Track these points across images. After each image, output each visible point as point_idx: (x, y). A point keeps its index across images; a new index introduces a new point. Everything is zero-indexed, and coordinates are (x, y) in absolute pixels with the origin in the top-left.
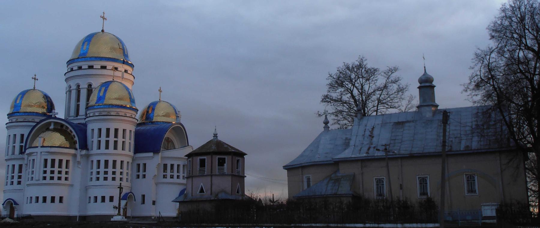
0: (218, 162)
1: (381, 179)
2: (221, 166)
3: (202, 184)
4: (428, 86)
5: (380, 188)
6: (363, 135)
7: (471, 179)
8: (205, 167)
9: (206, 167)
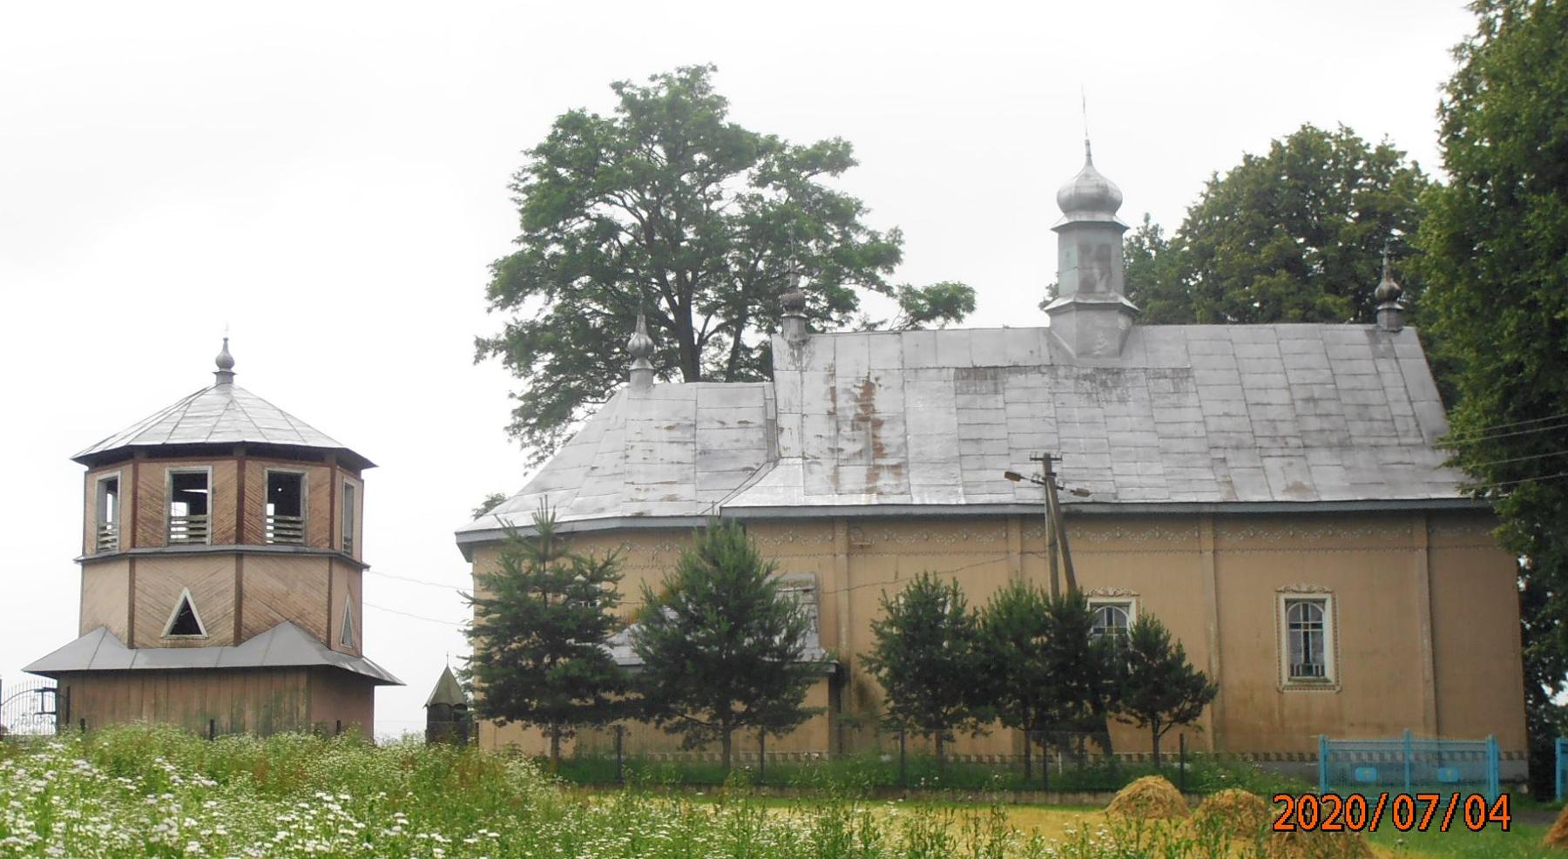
0: (269, 492)
1: (1310, 604)
2: (286, 514)
3: (186, 593)
4: (1103, 222)
5: (1306, 641)
6: (831, 414)
7: (1306, 619)
8: (205, 512)
9: (209, 511)
